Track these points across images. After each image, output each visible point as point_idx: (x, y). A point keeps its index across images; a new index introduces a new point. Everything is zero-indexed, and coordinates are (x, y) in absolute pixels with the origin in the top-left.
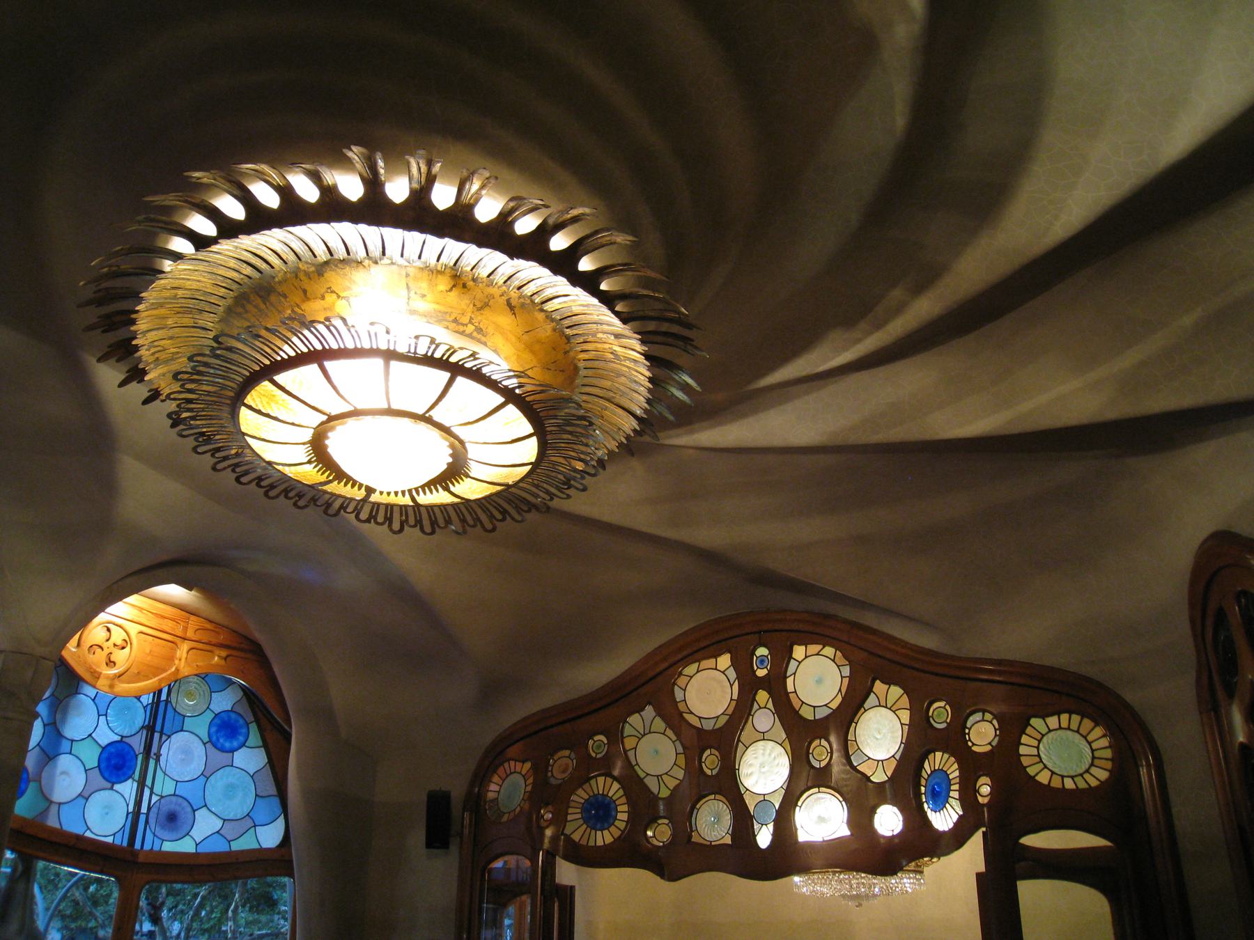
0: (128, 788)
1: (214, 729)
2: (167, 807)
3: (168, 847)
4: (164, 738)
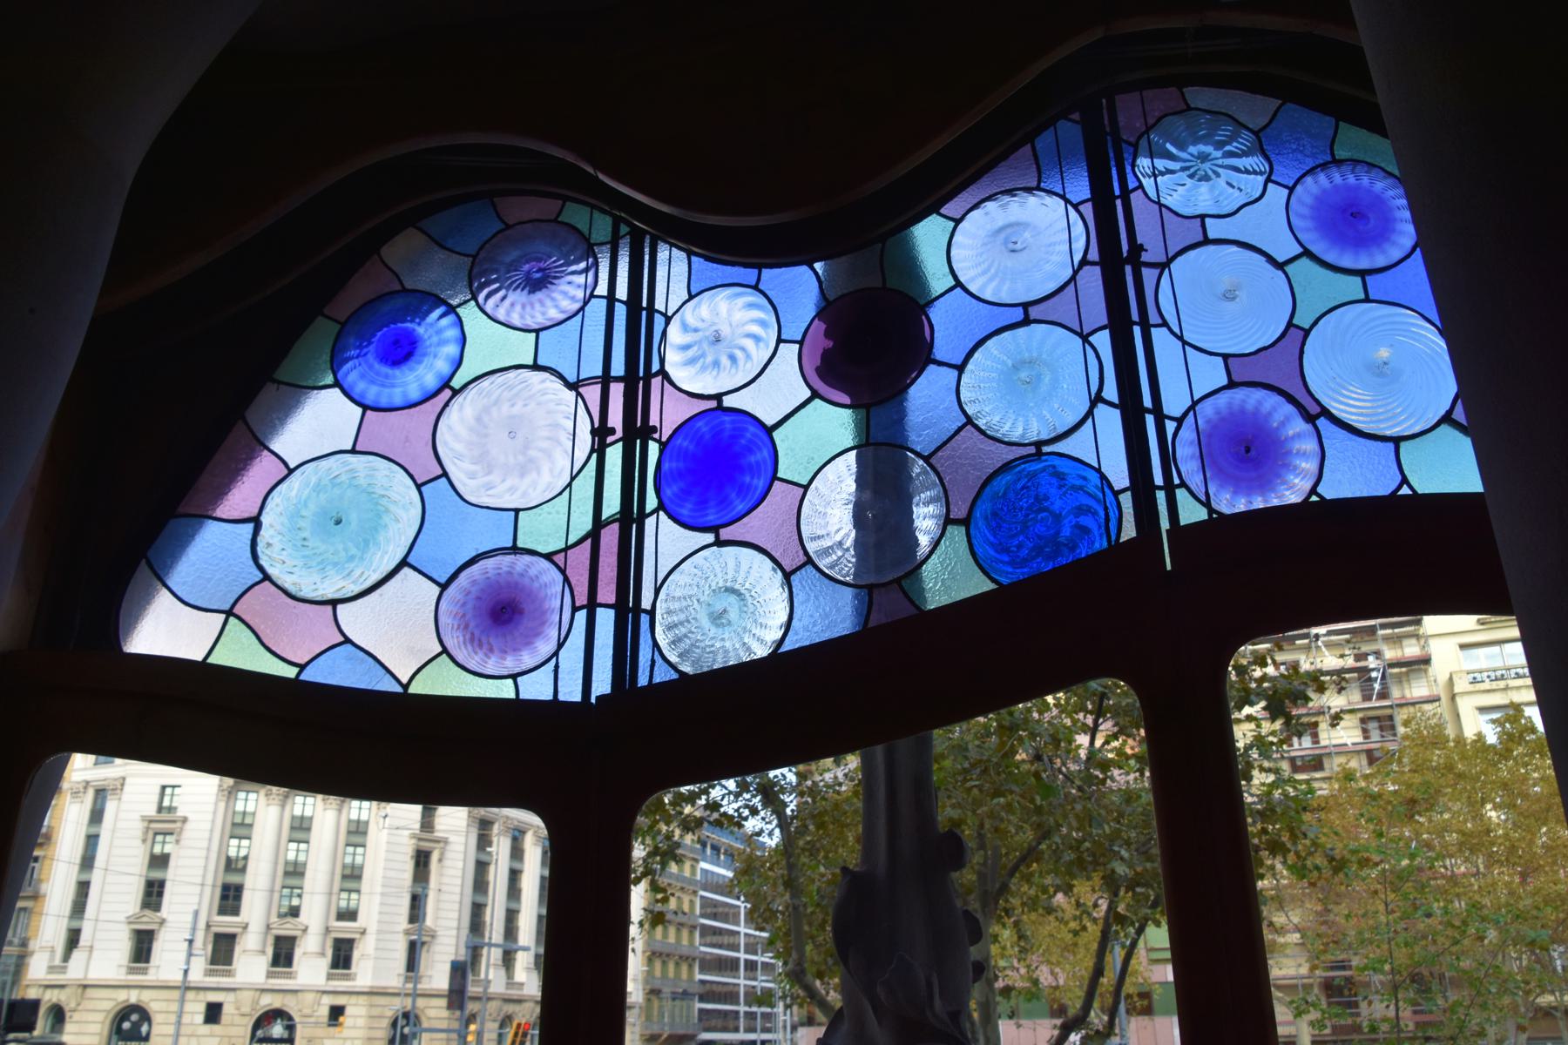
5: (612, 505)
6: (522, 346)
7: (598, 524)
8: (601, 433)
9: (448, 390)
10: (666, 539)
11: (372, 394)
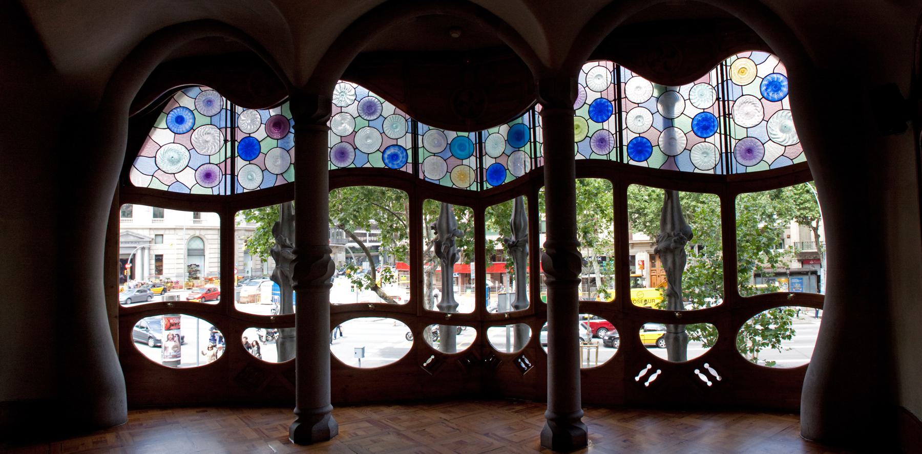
0: (715, 139)
1: (764, 88)
2: (743, 146)
3: (750, 170)
4: (731, 103)
5: (229, 154)
6: (208, 120)
7: (226, 159)
8: (226, 141)
9: (192, 129)
10: (240, 162)
11: (175, 131)
